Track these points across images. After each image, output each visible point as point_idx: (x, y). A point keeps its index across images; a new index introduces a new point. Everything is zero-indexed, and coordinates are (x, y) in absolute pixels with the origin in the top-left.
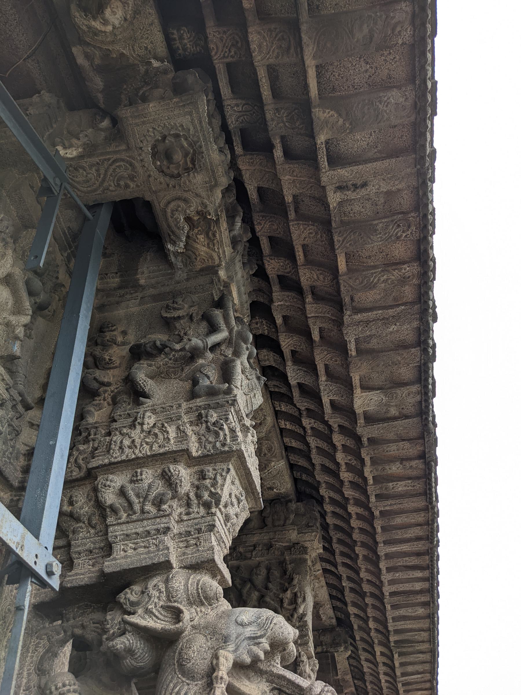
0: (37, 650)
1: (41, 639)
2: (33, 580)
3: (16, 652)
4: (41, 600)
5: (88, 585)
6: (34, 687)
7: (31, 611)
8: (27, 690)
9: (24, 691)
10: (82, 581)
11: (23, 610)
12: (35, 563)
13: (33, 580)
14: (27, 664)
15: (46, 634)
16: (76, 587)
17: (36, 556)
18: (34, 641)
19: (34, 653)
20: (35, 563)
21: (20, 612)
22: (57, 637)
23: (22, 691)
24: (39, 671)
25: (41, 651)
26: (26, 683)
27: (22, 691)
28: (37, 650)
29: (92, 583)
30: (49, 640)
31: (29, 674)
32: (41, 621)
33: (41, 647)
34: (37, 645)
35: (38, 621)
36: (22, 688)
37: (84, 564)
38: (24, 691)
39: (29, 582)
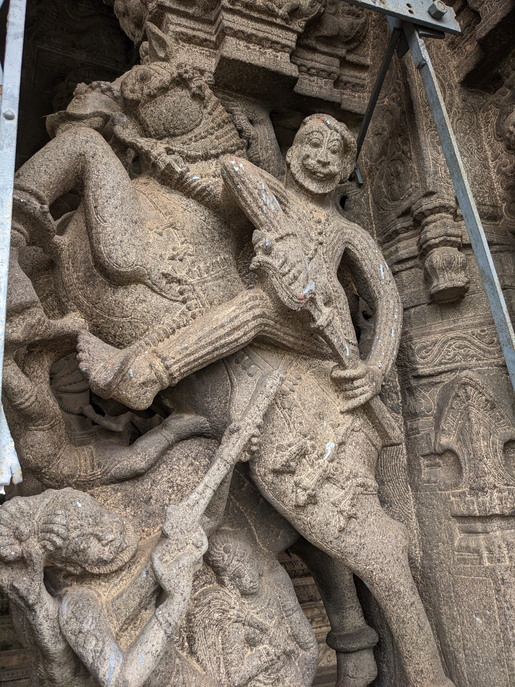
0: (489, 122)
1: (487, 111)
2: (421, 32)
3: (439, 104)
4: (465, 72)
5: (504, 18)
6: (502, 152)
7: (460, 90)
8: (495, 159)
9: (492, 161)
10: (496, 19)
11: (426, 64)
12: (411, 12)
13: (421, 32)
14: (484, 139)
15: (491, 103)
16: (492, 30)
17: (408, 5)
18: (481, 116)
19: (487, 126)
20: (411, 12)
21: (424, 70)
22: (504, 98)
23: (490, 162)
24: (500, 137)
25: (494, 120)
26: (492, 154)
27: (490, 162)
28: (489, 122)
29: (508, 12)
30: (497, 106)
31: (491, 146)
32: (481, 97)
33: (491, 117)
34: (487, 118)
35: (476, 98)
36: (489, 160)
37: (491, 5)
38: (492, 161)
39: (418, 38)
